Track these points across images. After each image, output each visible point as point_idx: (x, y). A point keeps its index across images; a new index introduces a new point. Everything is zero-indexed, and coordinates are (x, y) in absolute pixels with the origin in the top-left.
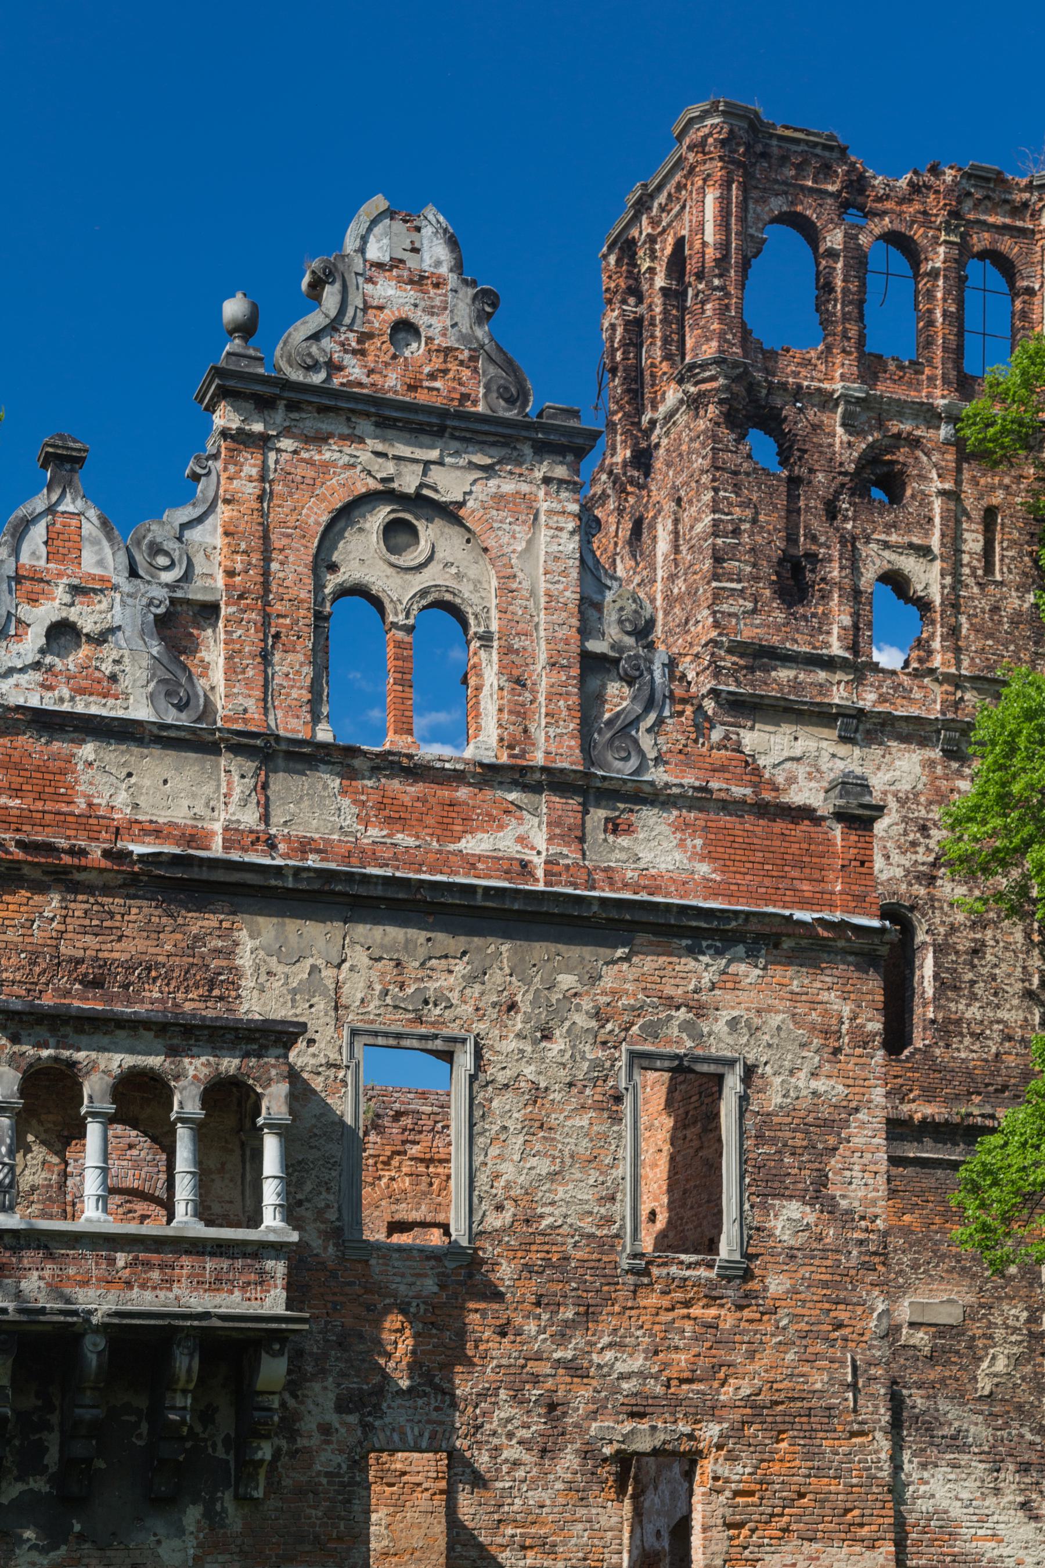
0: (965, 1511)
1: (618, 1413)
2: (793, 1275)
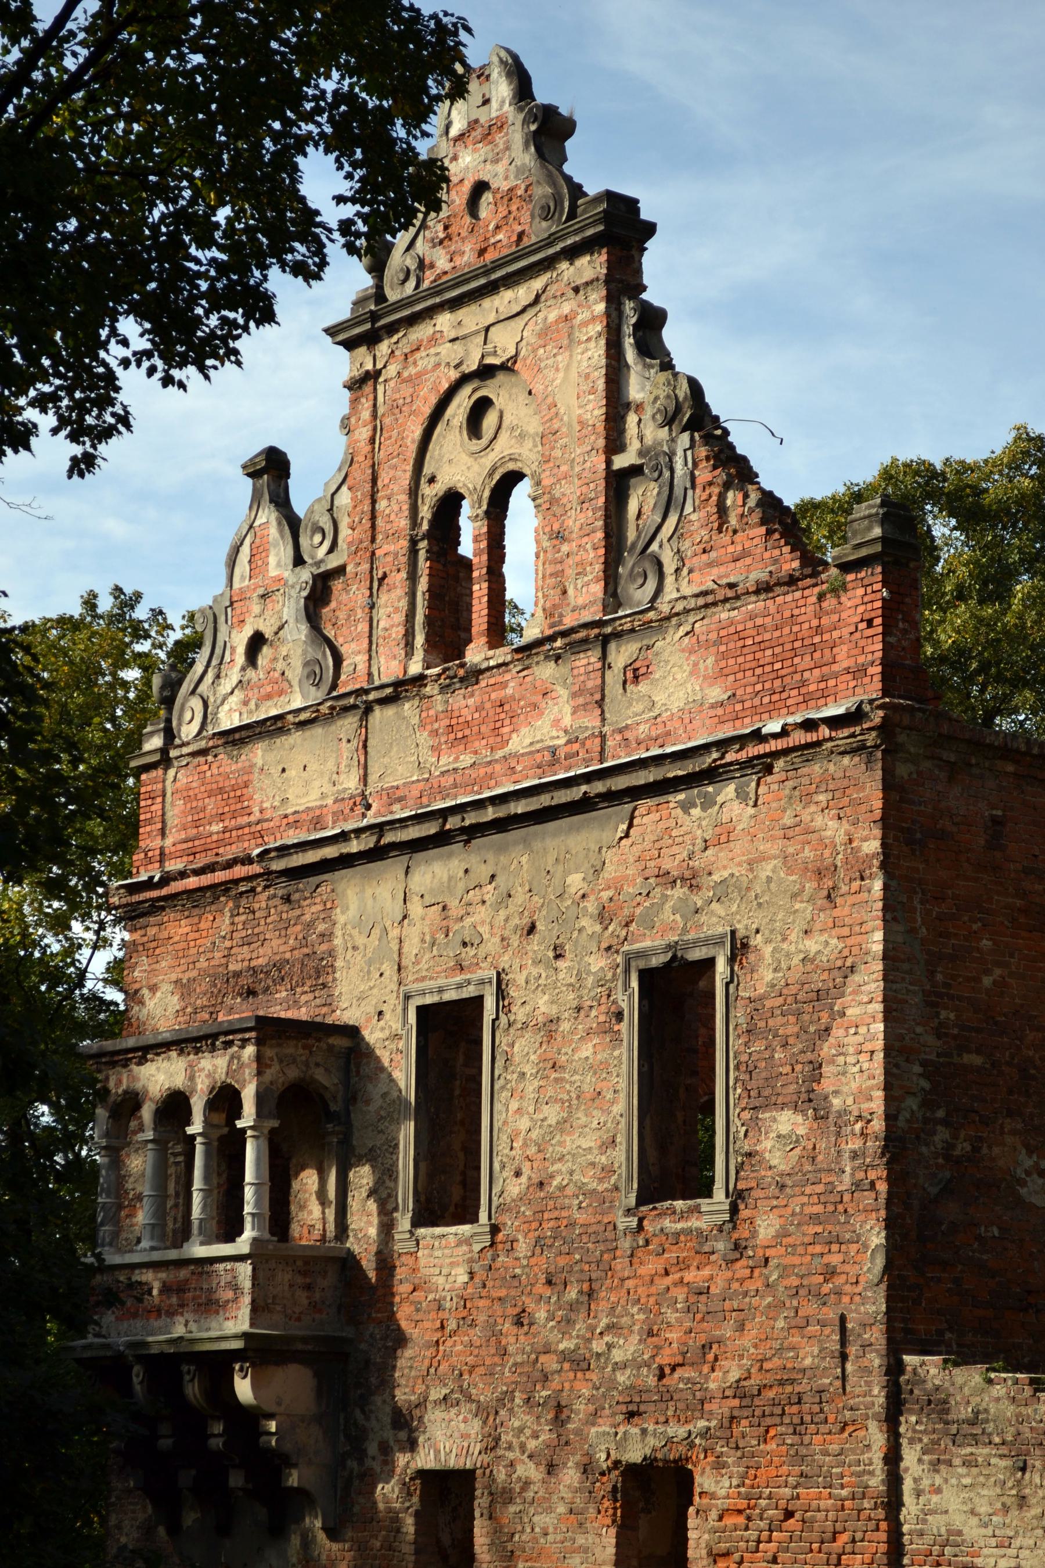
0: (983, 1531)
1: (613, 1415)
2: (783, 1211)
